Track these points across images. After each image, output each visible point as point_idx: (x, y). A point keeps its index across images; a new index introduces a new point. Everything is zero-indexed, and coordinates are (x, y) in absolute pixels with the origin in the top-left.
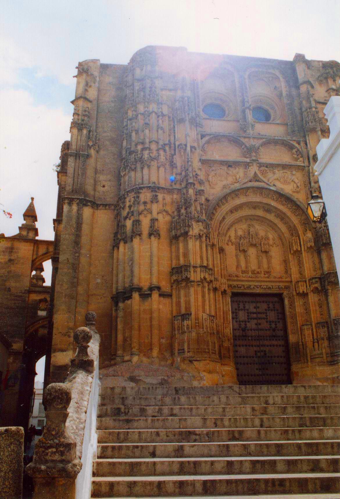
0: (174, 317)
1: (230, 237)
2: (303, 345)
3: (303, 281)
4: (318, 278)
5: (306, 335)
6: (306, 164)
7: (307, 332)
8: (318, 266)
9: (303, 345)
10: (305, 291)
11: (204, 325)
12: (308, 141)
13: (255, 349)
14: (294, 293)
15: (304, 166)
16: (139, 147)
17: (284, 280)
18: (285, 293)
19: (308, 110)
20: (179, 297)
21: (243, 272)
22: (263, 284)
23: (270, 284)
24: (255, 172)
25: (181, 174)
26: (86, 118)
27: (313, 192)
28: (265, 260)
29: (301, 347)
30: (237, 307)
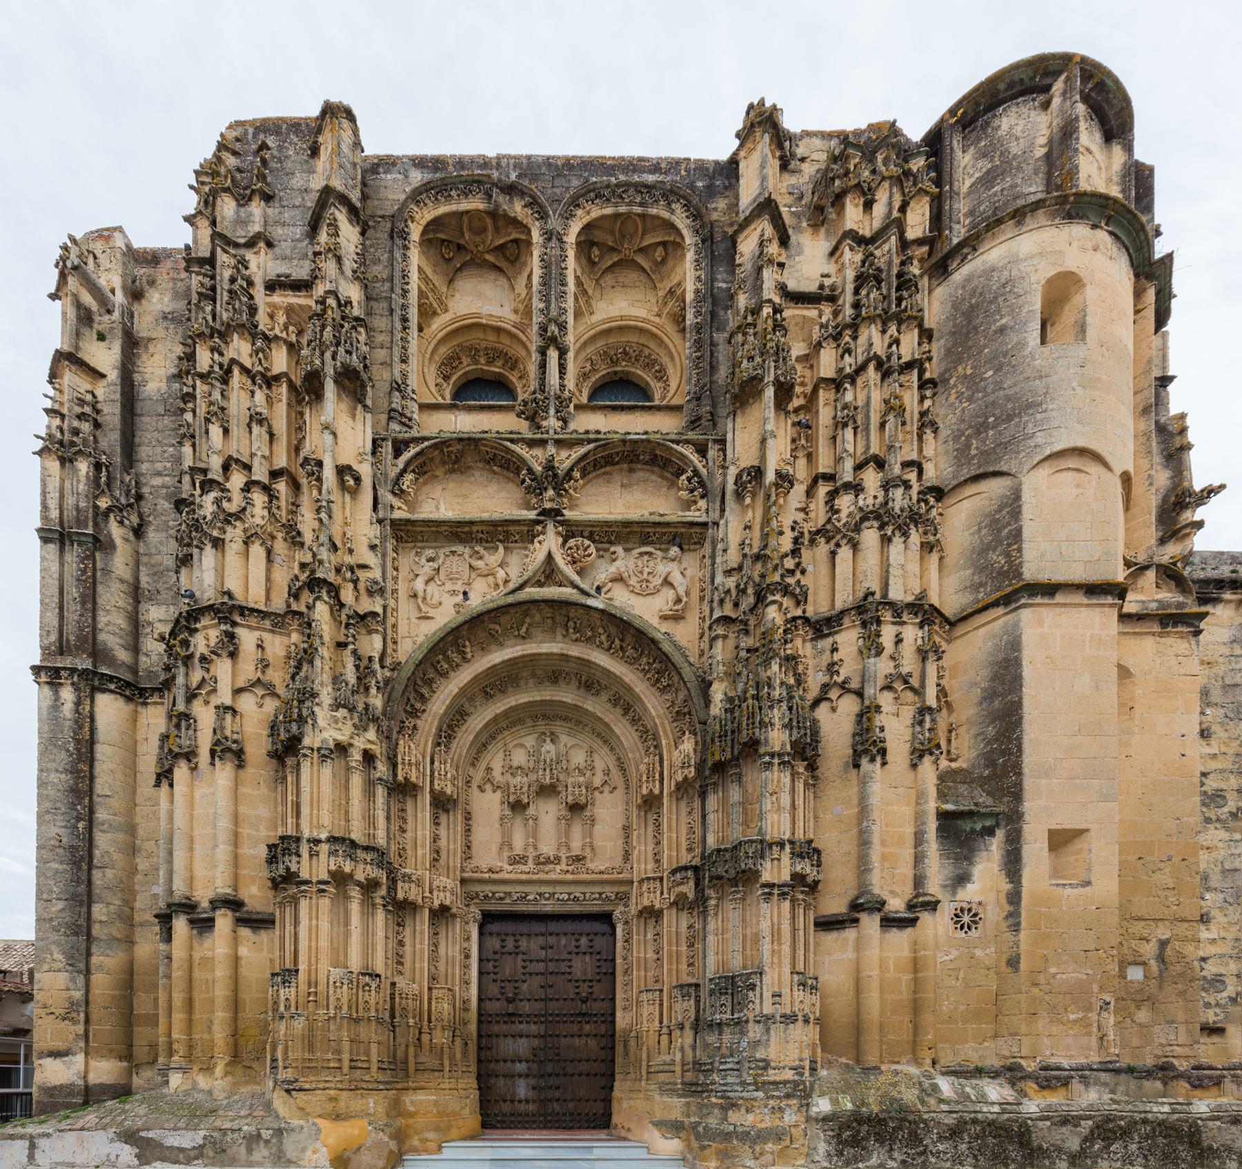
1: (489, 769)
13: (536, 1042)
21: (516, 860)
26: (86, 427)
30: (498, 947)
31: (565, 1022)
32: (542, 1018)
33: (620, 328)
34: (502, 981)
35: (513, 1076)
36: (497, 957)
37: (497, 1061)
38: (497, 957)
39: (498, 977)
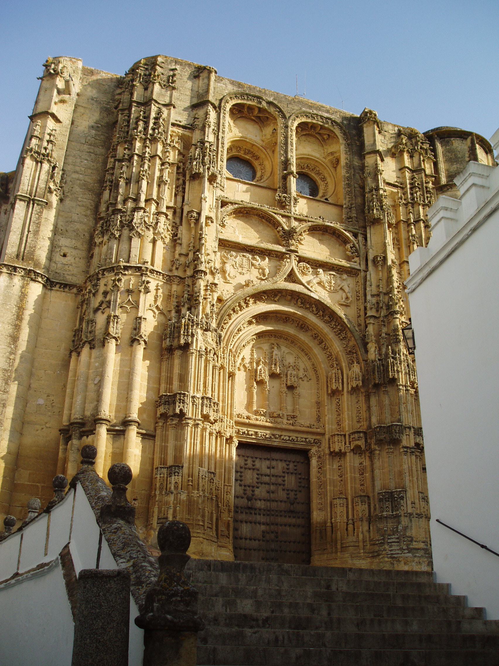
0: (157, 468)
2: (332, 527)
3: (341, 435)
4: (363, 432)
5: (338, 513)
6: (363, 267)
7: (340, 510)
8: (364, 415)
9: (332, 527)
10: (343, 451)
11: (201, 485)
12: (368, 235)
13: (263, 527)
14: (327, 451)
15: (360, 270)
16: (130, 205)
17: (315, 430)
18: (314, 450)
19: (374, 192)
20: (165, 439)
22: (284, 433)
23: (294, 436)
24: (292, 269)
25: (187, 255)
27: (368, 308)
28: (289, 399)
29: (329, 529)
31: (281, 516)
32: (268, 512)
33: (308, 158)
34: (245, 486)
35: (250, 550)
36: (242, 470)
37: (241, 539)
38: (242, 470)
39: (243, 483)
